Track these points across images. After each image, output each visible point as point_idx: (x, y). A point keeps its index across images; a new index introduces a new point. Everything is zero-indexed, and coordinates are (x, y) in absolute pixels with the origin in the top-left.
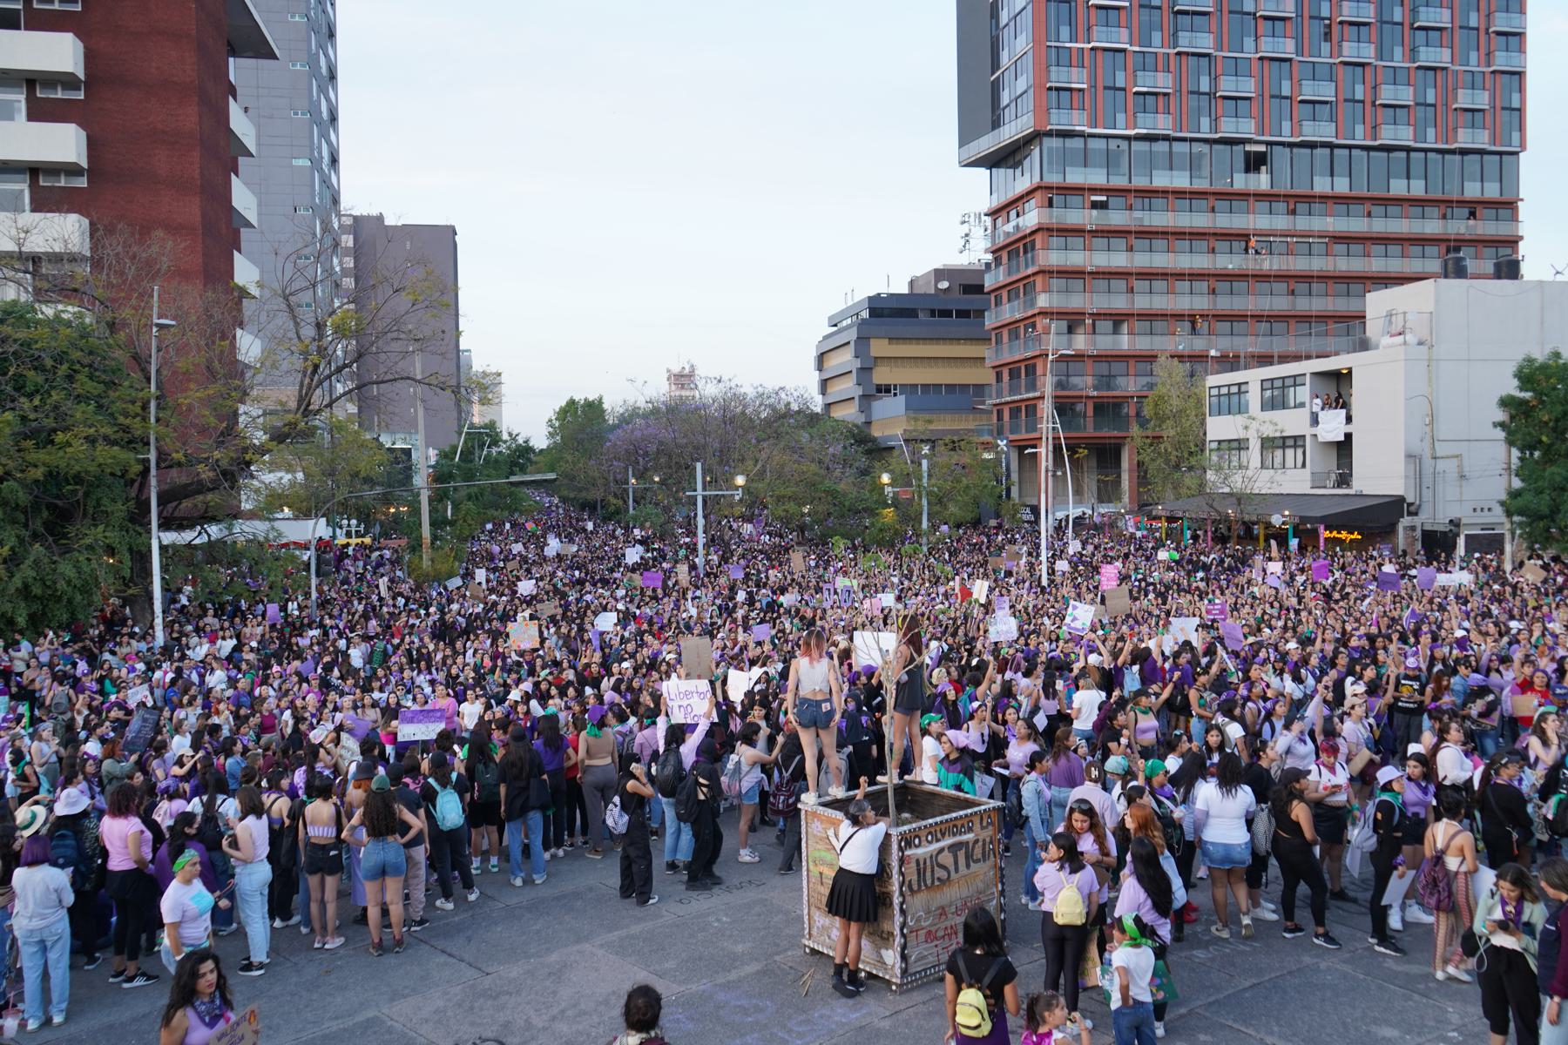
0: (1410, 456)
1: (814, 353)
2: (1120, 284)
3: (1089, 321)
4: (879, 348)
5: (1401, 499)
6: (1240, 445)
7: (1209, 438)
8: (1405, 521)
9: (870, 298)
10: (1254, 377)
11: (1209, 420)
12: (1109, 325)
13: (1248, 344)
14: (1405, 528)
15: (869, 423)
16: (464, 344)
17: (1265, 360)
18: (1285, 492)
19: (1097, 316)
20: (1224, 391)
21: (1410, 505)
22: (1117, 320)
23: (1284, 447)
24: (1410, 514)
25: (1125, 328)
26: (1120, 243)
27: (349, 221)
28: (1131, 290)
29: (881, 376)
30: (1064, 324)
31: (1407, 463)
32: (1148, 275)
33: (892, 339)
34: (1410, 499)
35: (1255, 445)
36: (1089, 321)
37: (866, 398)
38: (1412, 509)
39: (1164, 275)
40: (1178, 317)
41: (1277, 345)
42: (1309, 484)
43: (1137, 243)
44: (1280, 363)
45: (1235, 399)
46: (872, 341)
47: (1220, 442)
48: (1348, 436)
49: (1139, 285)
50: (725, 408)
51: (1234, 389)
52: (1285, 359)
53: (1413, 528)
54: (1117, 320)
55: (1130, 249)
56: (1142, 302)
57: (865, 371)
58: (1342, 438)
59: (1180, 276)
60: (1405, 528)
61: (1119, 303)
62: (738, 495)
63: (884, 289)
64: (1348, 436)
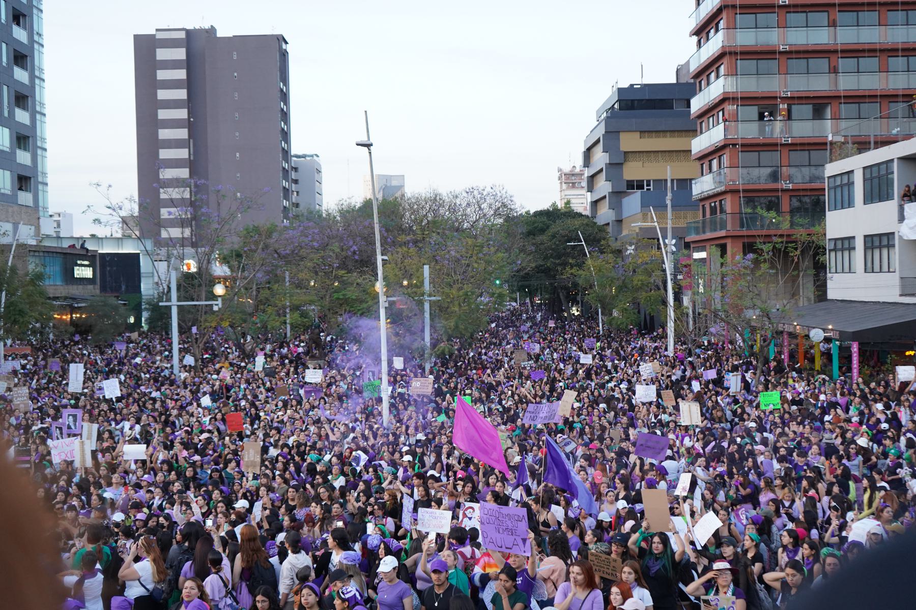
1: (583, 149)
2: (823, 63)
3: (783, 106)
4: (630, 142)
6: (846, 244)
7: (828, 236)
9: (619, 89)
10: (857, 163)
11: (828, 214)
12: (807, 109)
13: (872, 128)
15: (619, 221)
16: (296, 148)
17: (863, 146)
18: (881, 300)
19: (795, 100)
20: (838, 183)
22: (819, 105)
23: (880, 247)
25: (828, 112)
26: (823, 17)
27: (182, 35)
28: (834, 70)
29: (633, 171)
30: (753, 111)
32: (854, 52)
33: (643, 133)
35: (859, 244)
37: (617, 195)
39: (871, 51)
40: (891, 97)
41: (872, 128)
43: (840, 17)
44: (876, 148)
45: (846, 189)
46: (622, 135)
47: (836, 240)
49: (842, 63)
51: (845, 181)
54: (819, 105)
55: (833, 24)
56: (847, 83)
57: (614, 167)
59: (892, 51)
61: (820, 84)
62: (217, 305)
63: (637, 80)
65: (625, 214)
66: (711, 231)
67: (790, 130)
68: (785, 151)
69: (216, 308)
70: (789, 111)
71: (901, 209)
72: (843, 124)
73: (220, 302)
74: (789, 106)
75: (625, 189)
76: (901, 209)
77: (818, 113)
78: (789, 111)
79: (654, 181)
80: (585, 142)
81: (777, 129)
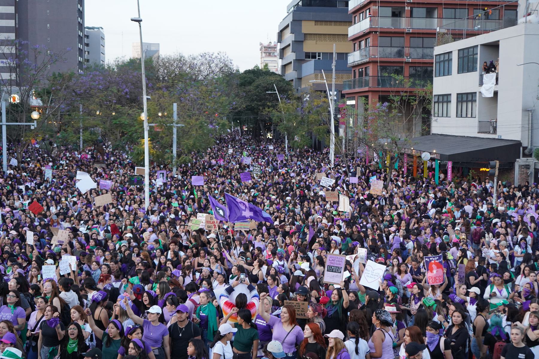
0: (526, 111)
1: (277, 31)
3: (408, 8)
4: (308, 27)
5: (518, 144)
6: (445, 98)
7: (435, 93)
8: (521, 161)
11: (435, 79)
12: (423, 11)
13: (464, 25)
14: (521, 166)
15: (300, 79)
16: (89, 21)
17: (457, 36)
18: (466, 135)
20: (442, 59)
21: (525, 148)
23: (467, 101)
24: (525, 155)
29: (309, 46)
31: (523, 116)
33: (317, 22)
34: (525, 144)
35: (454, 99)
36: (408, 8)
37: (299, 62)
38: (527, 151)
41: (464, 25)
42: (477, 131)
45: (446, 63)
46: (304, 23)
47: (439, 96)
48: (496, 93)
50: (118, 66)
51: (446, 58)
52: (470, 35)
53: (527, 167)
57: (298, 43)
58: (492, 95)
60: (521, 166)
62: (33, 126)
64: (496, 93)
65: (304, 74)
66: (359, 87)
67: (411, 24)
68: (407, 38)
69: (32, 128)
70: (411, 12)
71: (481, 76)
72: (445, 22)
73: (35, 123)
74: (411, 8)
75: (304, 58)
76: (481, 76)
77: (429, 14)
78: (411, 12)
79: (323, 53)
80: (279, 26)
81: (404, 24)
